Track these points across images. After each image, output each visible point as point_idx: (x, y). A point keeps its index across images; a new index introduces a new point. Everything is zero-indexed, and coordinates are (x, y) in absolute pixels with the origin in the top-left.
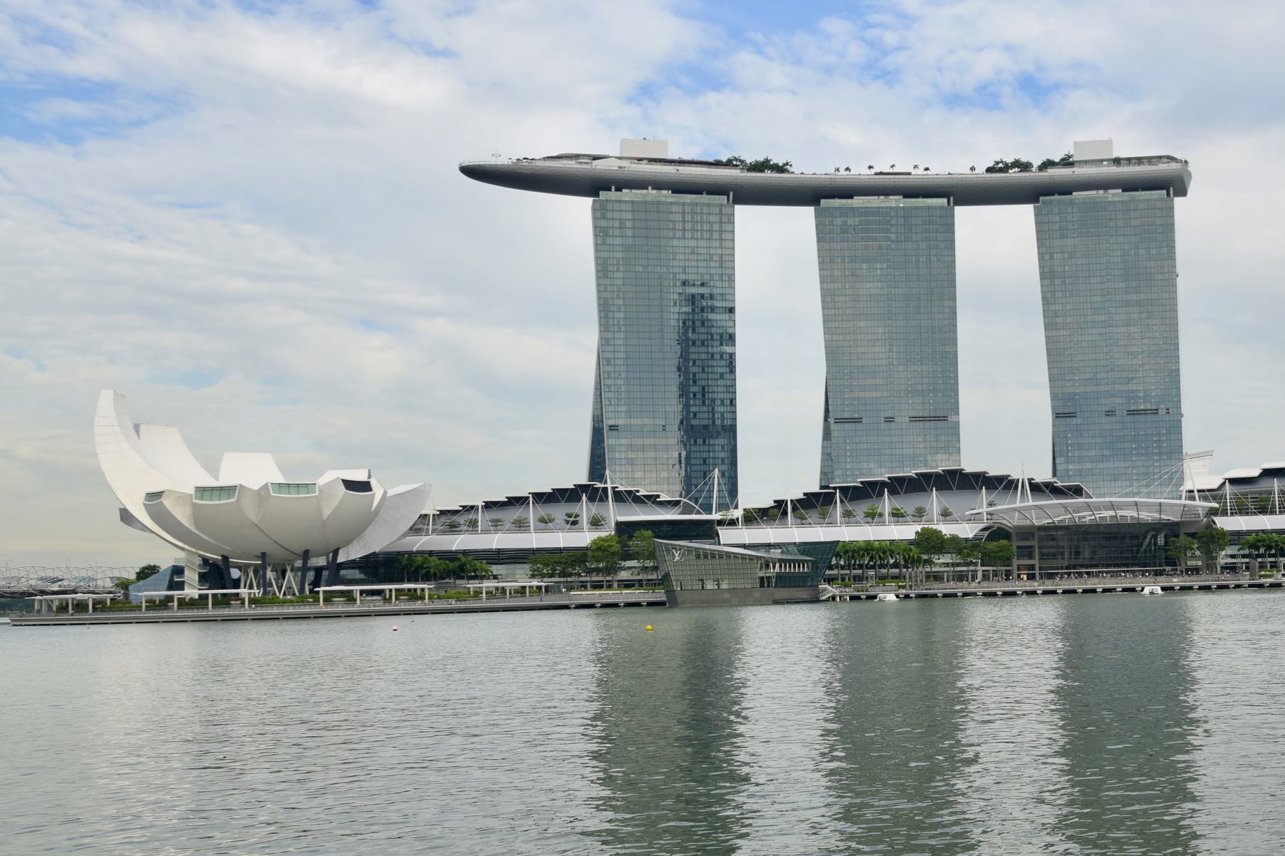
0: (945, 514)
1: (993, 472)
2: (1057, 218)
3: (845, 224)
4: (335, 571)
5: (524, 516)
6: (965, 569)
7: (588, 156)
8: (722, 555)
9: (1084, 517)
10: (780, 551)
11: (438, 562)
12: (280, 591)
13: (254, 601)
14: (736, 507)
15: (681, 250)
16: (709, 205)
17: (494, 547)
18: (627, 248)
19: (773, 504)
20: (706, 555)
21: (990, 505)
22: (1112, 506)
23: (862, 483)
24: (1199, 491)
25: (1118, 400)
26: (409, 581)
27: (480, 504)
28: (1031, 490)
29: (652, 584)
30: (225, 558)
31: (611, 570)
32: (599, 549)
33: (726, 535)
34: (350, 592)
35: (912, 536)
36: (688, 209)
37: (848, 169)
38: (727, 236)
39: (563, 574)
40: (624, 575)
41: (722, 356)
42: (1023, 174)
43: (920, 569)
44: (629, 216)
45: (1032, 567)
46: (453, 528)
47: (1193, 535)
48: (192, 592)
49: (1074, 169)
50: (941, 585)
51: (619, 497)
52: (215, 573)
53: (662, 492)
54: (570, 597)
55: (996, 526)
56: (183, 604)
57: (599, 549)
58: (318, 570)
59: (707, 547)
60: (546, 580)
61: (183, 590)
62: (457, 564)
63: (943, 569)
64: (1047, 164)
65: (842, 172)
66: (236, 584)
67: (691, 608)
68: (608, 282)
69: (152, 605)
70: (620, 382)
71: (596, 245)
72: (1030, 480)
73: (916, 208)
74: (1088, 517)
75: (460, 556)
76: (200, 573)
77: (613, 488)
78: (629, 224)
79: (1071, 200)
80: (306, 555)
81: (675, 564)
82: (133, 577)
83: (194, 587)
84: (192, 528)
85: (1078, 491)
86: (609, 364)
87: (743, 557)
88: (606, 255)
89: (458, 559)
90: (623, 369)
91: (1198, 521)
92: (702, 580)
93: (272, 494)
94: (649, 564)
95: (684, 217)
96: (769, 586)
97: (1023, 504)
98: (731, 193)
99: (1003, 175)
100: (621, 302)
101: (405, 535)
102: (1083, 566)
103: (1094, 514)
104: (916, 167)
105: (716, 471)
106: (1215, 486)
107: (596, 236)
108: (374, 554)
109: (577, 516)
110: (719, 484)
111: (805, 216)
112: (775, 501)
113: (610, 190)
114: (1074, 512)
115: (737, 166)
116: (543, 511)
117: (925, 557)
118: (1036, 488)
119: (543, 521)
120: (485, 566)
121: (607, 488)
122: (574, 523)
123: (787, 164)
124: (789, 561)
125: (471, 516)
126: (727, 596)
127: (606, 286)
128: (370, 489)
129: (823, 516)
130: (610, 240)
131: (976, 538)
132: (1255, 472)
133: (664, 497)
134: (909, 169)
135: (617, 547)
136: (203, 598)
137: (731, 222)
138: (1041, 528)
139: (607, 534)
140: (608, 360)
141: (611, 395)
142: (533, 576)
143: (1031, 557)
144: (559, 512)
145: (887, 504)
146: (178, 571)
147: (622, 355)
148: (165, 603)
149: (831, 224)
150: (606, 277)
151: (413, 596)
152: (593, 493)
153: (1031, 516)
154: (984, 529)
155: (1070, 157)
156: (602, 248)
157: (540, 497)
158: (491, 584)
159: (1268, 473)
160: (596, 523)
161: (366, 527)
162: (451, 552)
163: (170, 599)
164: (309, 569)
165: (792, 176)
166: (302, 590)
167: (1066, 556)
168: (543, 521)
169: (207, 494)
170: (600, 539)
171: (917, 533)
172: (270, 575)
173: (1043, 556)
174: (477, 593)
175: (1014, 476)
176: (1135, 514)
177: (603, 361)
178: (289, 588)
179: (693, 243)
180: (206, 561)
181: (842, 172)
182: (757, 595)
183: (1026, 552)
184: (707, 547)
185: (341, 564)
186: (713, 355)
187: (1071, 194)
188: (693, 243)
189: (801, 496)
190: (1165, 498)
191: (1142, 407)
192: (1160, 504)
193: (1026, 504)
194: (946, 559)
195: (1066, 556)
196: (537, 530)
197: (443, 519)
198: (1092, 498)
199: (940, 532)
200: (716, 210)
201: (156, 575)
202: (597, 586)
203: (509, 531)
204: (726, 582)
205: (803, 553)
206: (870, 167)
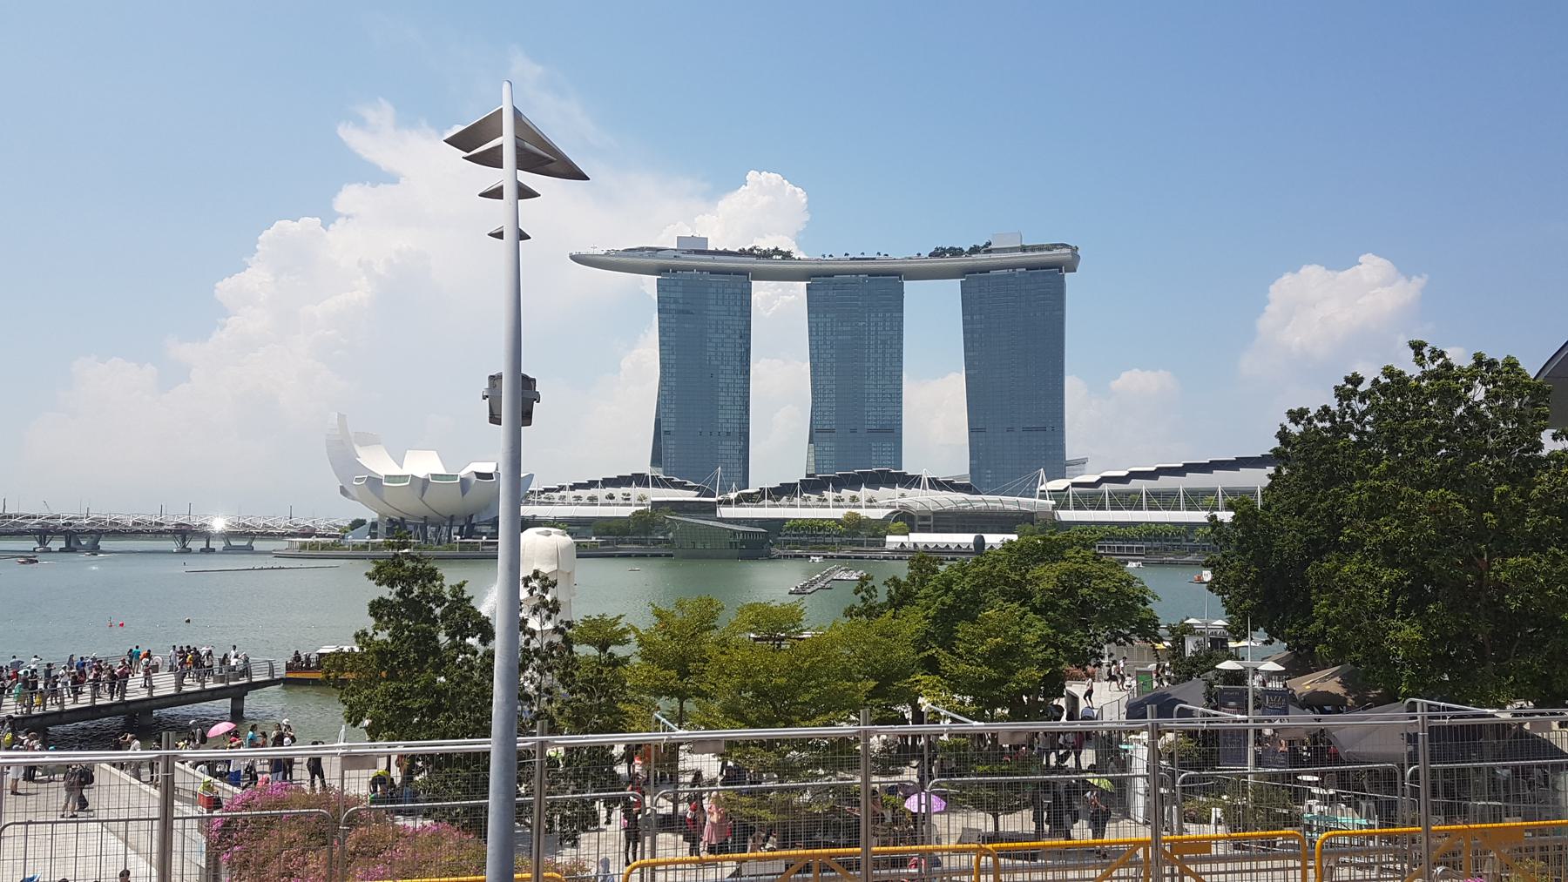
14: (732, 492)
33: (725, 512)
37: (831, 256)
79: (989, 277)
80: (452, 518)
93: (408, 483)
105: (719, 468)
106: (1062, 488)
110: (721, 476)
118: (936, 484)
125: (562, 493)
132: (1094, 479)
144: (618, 492)
145: (830, 495)
146: (374, 525)
152: (640, 480)
157: (607, 482)
159: (1104, 480)
176: (1001, 505)
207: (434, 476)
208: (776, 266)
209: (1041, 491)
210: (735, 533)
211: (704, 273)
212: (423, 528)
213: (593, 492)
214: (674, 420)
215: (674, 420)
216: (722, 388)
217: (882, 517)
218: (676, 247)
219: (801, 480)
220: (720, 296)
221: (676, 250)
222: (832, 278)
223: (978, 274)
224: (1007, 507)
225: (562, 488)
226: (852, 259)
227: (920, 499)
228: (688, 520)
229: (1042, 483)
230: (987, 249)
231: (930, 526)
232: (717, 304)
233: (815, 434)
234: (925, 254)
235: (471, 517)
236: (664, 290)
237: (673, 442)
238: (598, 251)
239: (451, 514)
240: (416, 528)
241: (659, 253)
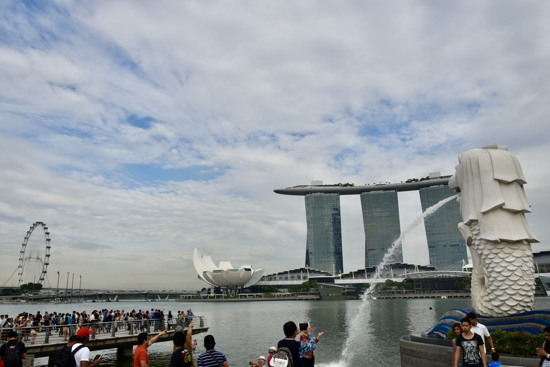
0: (395, 276)
1: (409, 263)
2: (426, 193)
3: (368, 198)
4: (243, 290)
5: (287, 276)
6: (399, 290)
7: (303, 186)
8: (334, 287)
9: (434, 276)
10: (348, 286)
11: (267, 288)
12: (231, 295)
13: (225, 297)
14: (339, 274)
15: (327, 207)
16: (333, 196)
17: (280, 284)
18: (313, 208)
19: (349, 273)
20: (331, 287)
21: (407, 273)
22: (441, 273)
23: (373, 267)
24: (467, 268)
25: (447, 242)
26: (260, 293)
27: (277, 273)
28: (419, 269)
29: (316, 294)
30: (219, 287)
31: (308, 290)
32: (304, 285)
33: (337, 281)
34: (246, 295)
35: (385, 282)
36: (328, 197)
38: (338, 203)
39: (296, 291)
40: (311, 292)
41: (338, 234)
42: (417, 183)
43: (387, 291)
44: (313, 200)
45: (420, 290)
46: (271, 279)
47: (465, 281)
48: (212, 295)
49: (430, 180)
50: (394, 295)
51: (310, 271)
52: (217, 290)
53: (321, 269)
54: (297, 297)
55: (409, 279)
56: (211, 297)
57: (304, 284)
58: (240, 290)
59: (332, 285)
60: (292, 293)
61: (210, 294)
62: (271, 288)
63: (394, 290)
64: (423, 179)
65: (367, 185)
66: (222, 293)
67: (326, 300)
68: (309, 216)
69: (204, 298)
70: (312, 241)
71: (306, 207)
72: (418, 266)
73: (387, 193)
74: (435, 276)
75: (272, 286)
76: (214, 291)
77: (308, 269)
78: (314, 202)
80: (237, 286)
81: (321, 289)
82: (201, 291)
83: (212, 293)
84: (212, 280)
85: (433, 269)
86: (310, 237)
87: (338, 287)
88: (308, 210)
89: (271, 287)
90: (313, 238)
91: (467, 277)
92: (328, 293)
94: (316, 289)
95: (327, 199)
96: (345, 295)
97: (416, 273)
98: (339, 193)
99: (410, 183)
100: (312, 221)
101: (259, 281)
102: (436, 290)
103: (436, 275)
104: (386, 182)
107: (306, 205)
108: (252, 286)
109: (300, 276)
111: (358, 197)
112: (350, 272)
113: (309, 194)
114: (431, 275)
115: (340, 186)
116: (292, 275)
117: (388, 287)
118: (420, 268)
119: (291, 277)
120: (277, 289)
121: (307, 269)
122: (299, 278)
123: (353, 184)
124: (350, 289)
125: (275, 276)
126: (334, 297)
127: (308, 217)
128: (251, 270)
129: (362, 276)
130: (309, 206)
131: (402, 282)
133: (322, 271)
134: (385, 183)
135: (308, 284)
136: (214, 296)
137: (339, 199)
138: (422, 279)
139: (306, 281)
140: (309, 236)
141: (310, 245)
142: (289, 292)
143: (420, 287)
144: (296, 275)
146: (209, 289)
147: (313, 234)
148: (206, 297)
149: (365, 199)
150: (308, 215)
151: (260, 296)
152: (303, 270)
153: (419, 276)
154: (405, 280)
155: (428, 177)
156: (307, 208)
157: (291, 272)
158: (279, 294)
160: (305, 278)
161: (249, 280)
162: (270, 285)
163: (207, 296)
164: (238, 289)
165: (354, 187)
166: (236, 294)
167: (430, 287)
168: (291, 277)
169: (215, 272)
170: (304, 282)
171: (386, 281)
172: (229, 291)
173: (423, 287)
174: (275, 296)
175: (415, 265)
177: (308, 236)
178: (233, 294)
179: (329, 206)
180: (215, 287)
181: (367, 185)
182: (342, 297)
183: (418, 286)
184: (332, 285)
185: (244, 288)
186: (335, 234)
187: (429, 187)
188: (329, 206)
189: (357, 271)
190: (457, 271)
191: (454, 244)
192: (455, 272)
193: (418, 273)
194: (394, 288)
195: (430, 287)
196: (290, 280)
197: (269, 277)
198: (438, 271)
199: (392, 281)
200: (335, 197)
201: (205, 291)
202: (304, 294)
203: (284, 280)
204: (334, 294)
205: (354, 286)
206: (374, 183)
207: (231, 270)
208: (349, 190)
209: (464, 269)
210: (344, 289)
211: (322, 193)
212: (227, 290)
213: (285, 276)
214: (313, 248)
215: (313, 248)
216: (331, 235)
217: (401, 281)
218: (311, 185)
219: (365, 268)
220: (328, 201)
221: (311, 186)
222: (369, 192)
223: (425, 188)
224: (451, 275)
225: (275, 274)
226: (376, 185)
227: (416, 274)
228: (325, 284)
229: (464, 265)
230: (428, 178)
231: (420, 284)
232: (327, 204)
233: (368, 251)
234: (404, 182)
235: (243, 286)
236: (307, 200)
237: (314, 256)
238: (283, 188)
239: (236, 284)
240: (224, 290)
241: (305, 187)
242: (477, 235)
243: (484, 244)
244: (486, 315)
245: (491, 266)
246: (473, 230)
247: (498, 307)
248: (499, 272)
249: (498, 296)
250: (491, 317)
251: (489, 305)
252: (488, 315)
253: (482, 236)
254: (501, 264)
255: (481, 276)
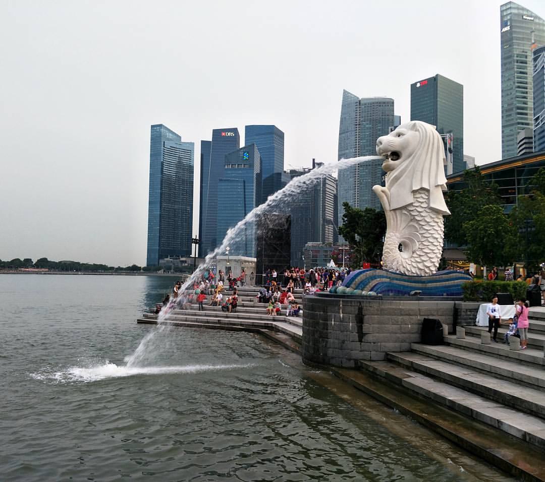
242: (422, 203)
243: (427, 212)
244: (413, 275)
245: (430, 232)
246: (417, 198)
247: (428, 267)
248: (437, 239)
249: (430, 258)
250: (418, 276)
251: (420, 266)
252: (415, 275)
253: (432, 205)
254: (439, 232)
255: (402, 240)
